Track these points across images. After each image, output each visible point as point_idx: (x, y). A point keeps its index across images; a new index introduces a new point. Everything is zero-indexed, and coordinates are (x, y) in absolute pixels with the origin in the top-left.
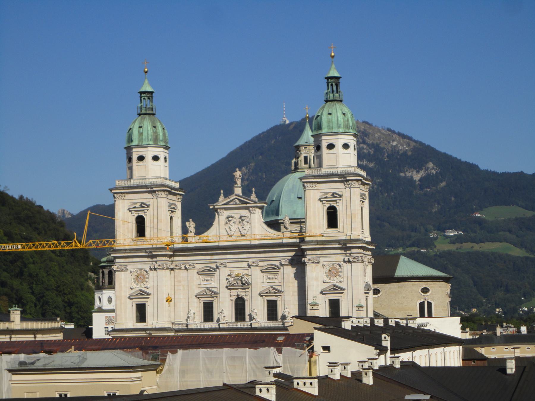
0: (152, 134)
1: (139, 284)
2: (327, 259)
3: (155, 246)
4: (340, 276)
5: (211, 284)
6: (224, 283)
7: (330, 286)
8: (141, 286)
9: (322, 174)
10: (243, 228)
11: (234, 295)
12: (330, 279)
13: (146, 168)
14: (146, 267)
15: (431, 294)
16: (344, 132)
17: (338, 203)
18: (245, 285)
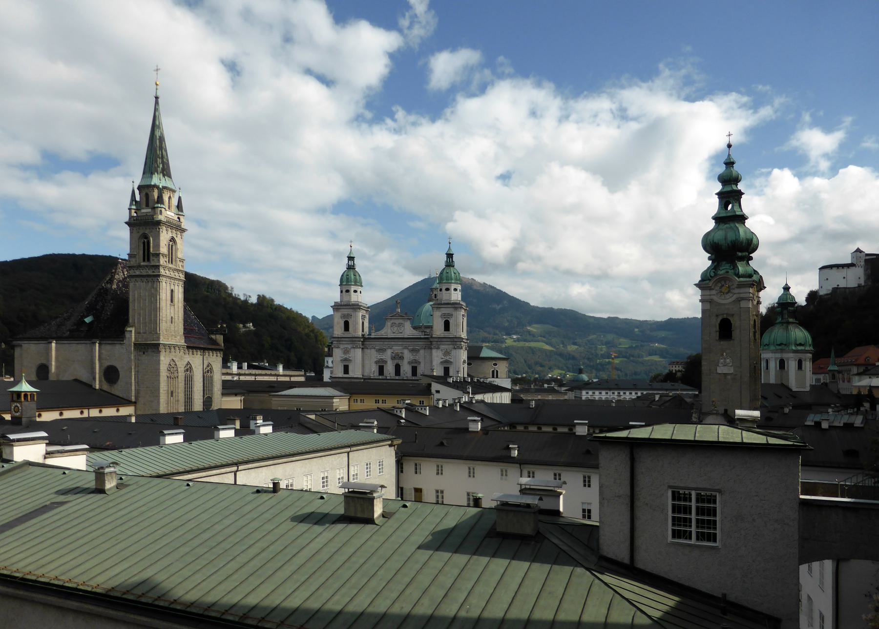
2: (443, 347)
6: (390, 356)
14: (349, 346)
18: (402, 358)
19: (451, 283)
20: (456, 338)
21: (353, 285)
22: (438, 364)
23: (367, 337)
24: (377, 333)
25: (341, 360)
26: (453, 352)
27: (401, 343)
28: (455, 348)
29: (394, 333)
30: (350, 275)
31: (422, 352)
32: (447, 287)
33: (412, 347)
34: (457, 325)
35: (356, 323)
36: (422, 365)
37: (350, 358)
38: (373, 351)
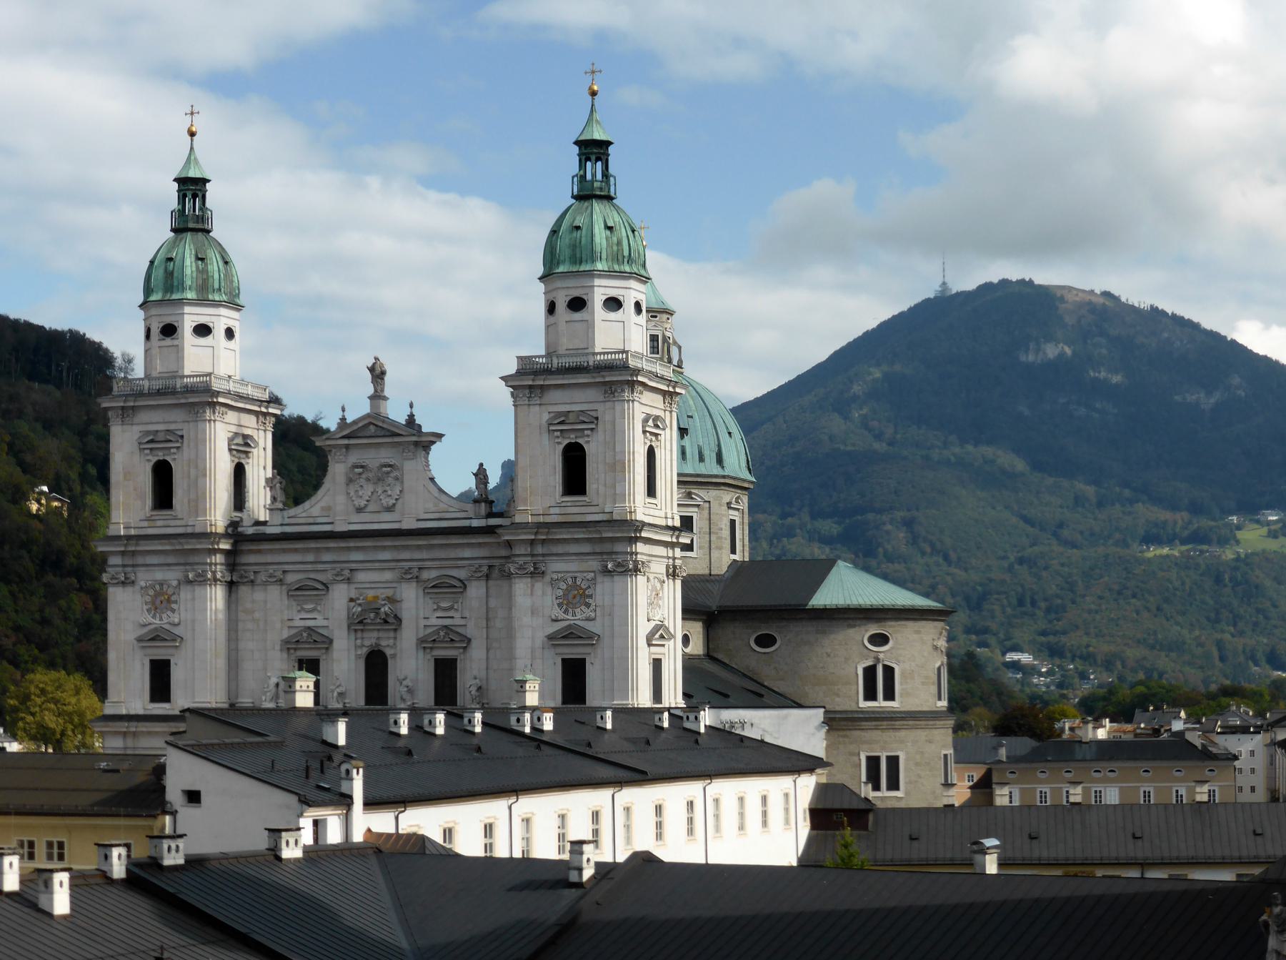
0: (194, 275)
1: (158, 615)
3: (189, 530)
4: (588, 605)
5: (315, 619)
7: (562, 629)
8: (161, 619)
9: (553, 369)
10: (385, 491)
11: (363, 646)
12: (566, 612)
13: (178, 352)
15: (892, 648)
16: (607, 269)
17: (588, 436)
18: (393, 622)
19: (591, 274)
20: (611, 523)
21: (192, 303)
22: (539, 643)
23: (250, 531)
24: (293, 511)
25: (139, 640)
26: (599, 587)
27: (386, 555)
28: (606, 572)
29: (360, 510)
30: (178, 261)
31: (476, 591)
32: (576, 293)
33: (434, 574)
34: (618, 467)
35: (200, 471)
36: (477, 652)
37: (176, 631)
38: (274, 595)
